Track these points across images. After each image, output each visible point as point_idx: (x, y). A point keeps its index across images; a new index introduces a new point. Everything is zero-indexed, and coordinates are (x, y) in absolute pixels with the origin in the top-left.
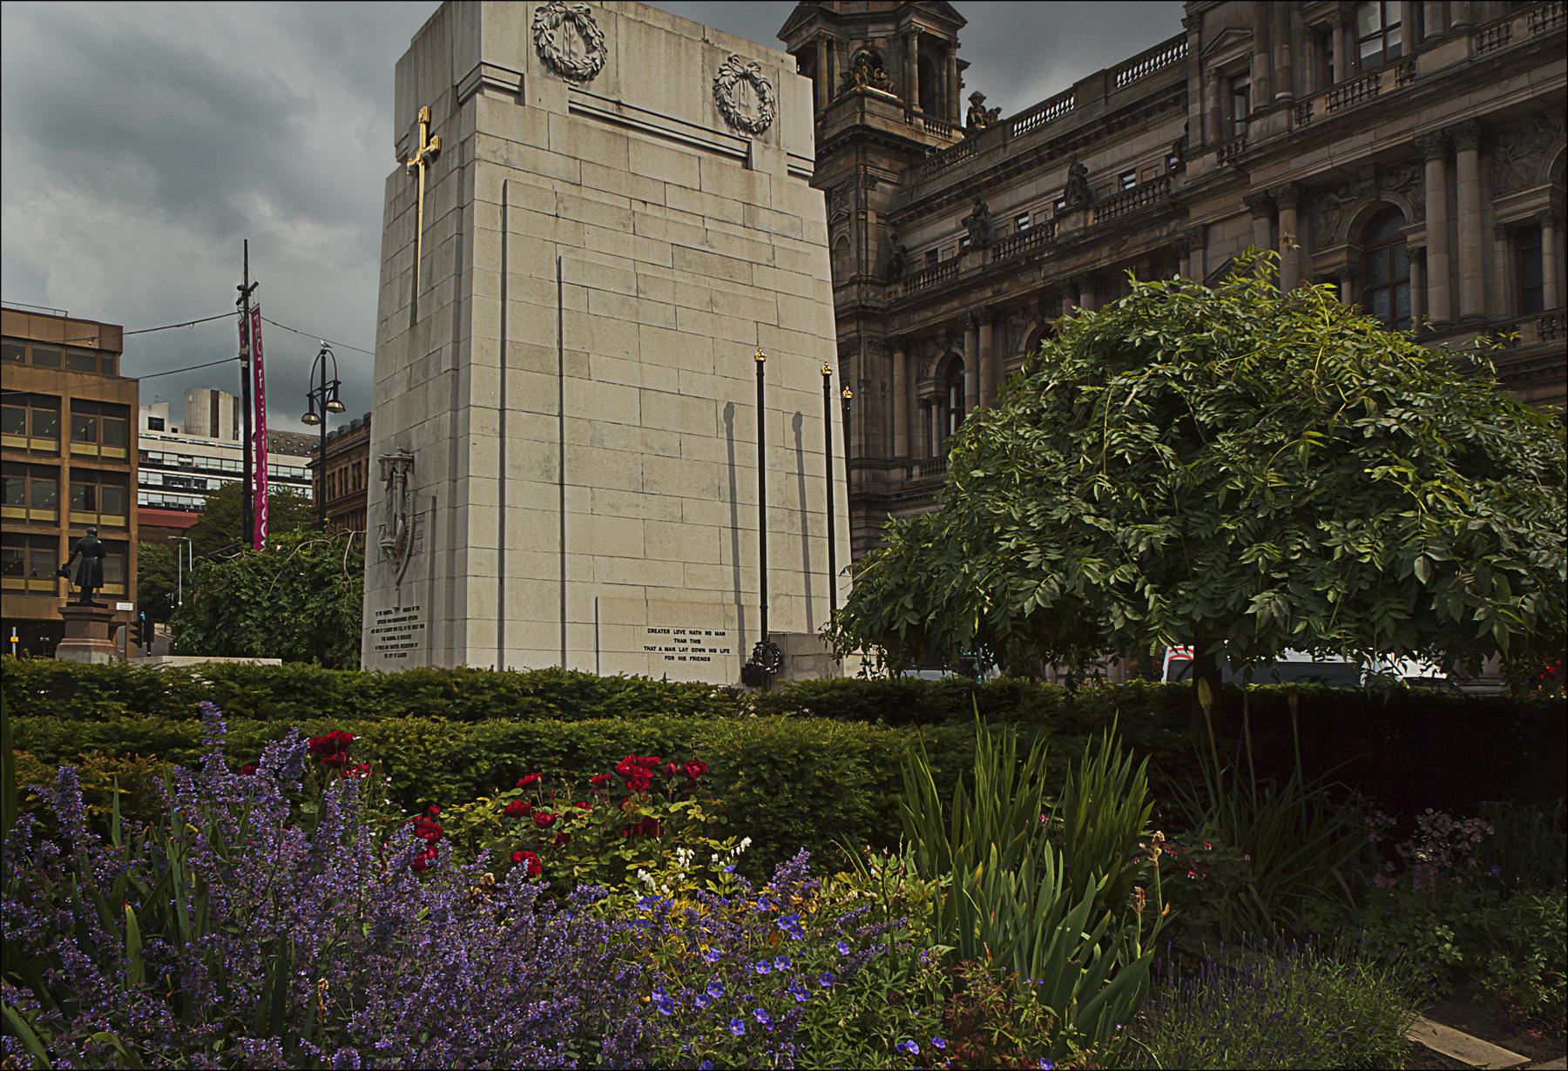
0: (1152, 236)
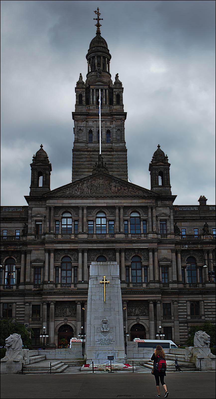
0: (15, 247)
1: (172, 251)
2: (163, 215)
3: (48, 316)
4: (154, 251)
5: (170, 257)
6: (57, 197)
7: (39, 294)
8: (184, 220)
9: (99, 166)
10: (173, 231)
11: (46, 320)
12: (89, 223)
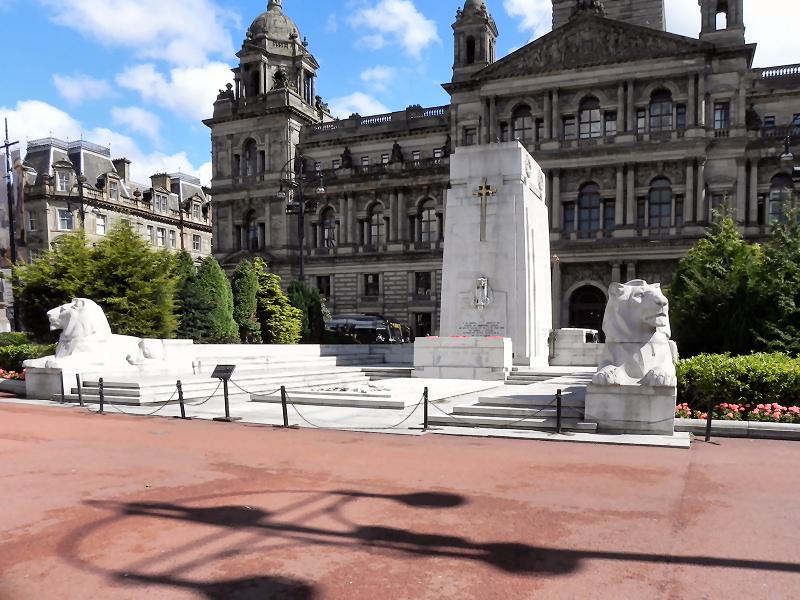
1: (739, 161)
2: (723, 89)
4: (696, 163)
5: (734, 175)
6: (499, 77)
8: (770, 97)
10: (742, 121)
12: (568, 122)
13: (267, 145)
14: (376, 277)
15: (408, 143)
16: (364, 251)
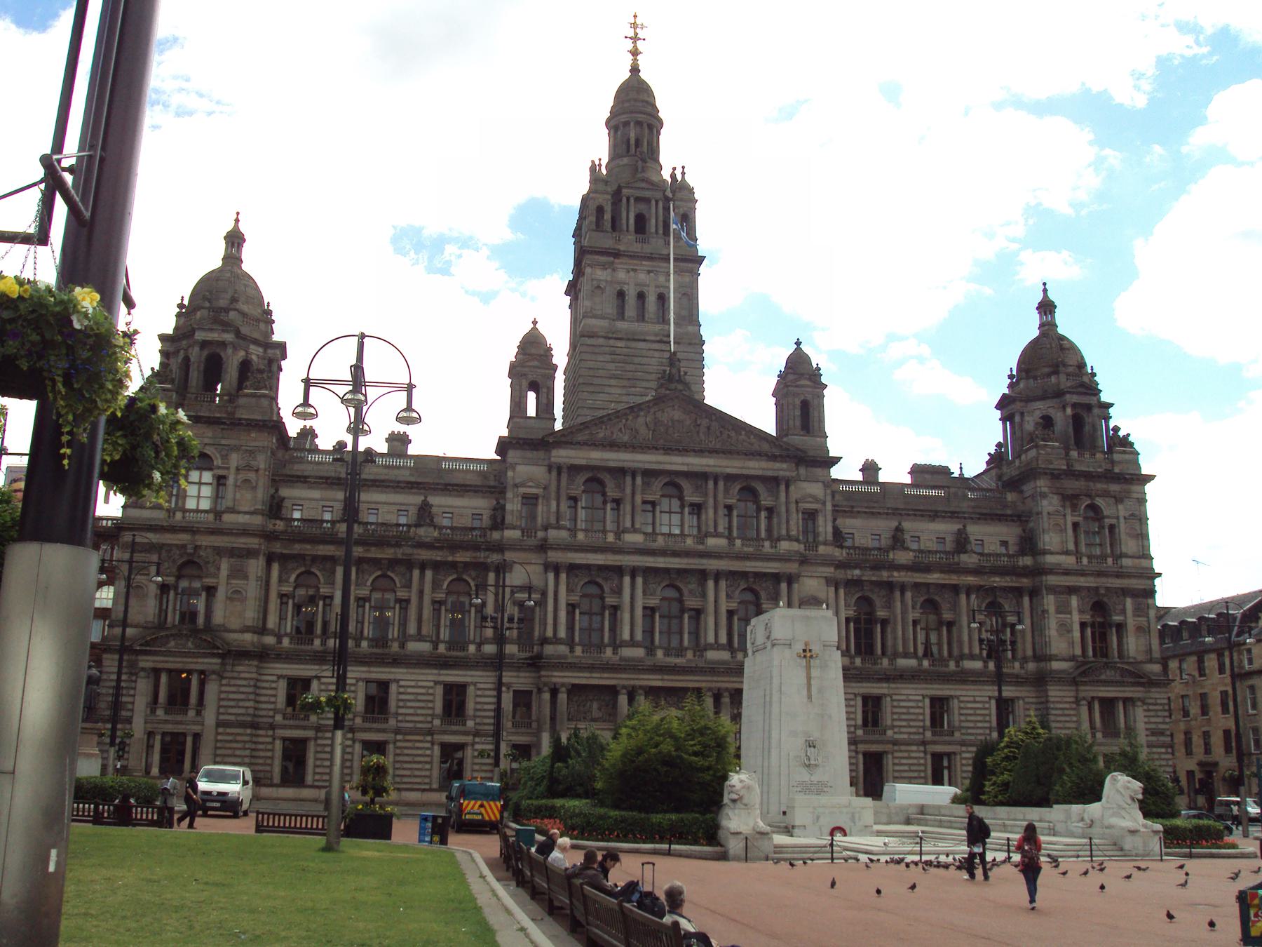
1: (829, 581)
3: (553, 719)
4: (790, 579)
7: (529, 665)
8: (851, 513)
9: (671, 379)
10: (830, 537)
11: (548, 726)
13: (233, 470)
14: (384, 686)
15: (435, 500)
16: (369, 647)
